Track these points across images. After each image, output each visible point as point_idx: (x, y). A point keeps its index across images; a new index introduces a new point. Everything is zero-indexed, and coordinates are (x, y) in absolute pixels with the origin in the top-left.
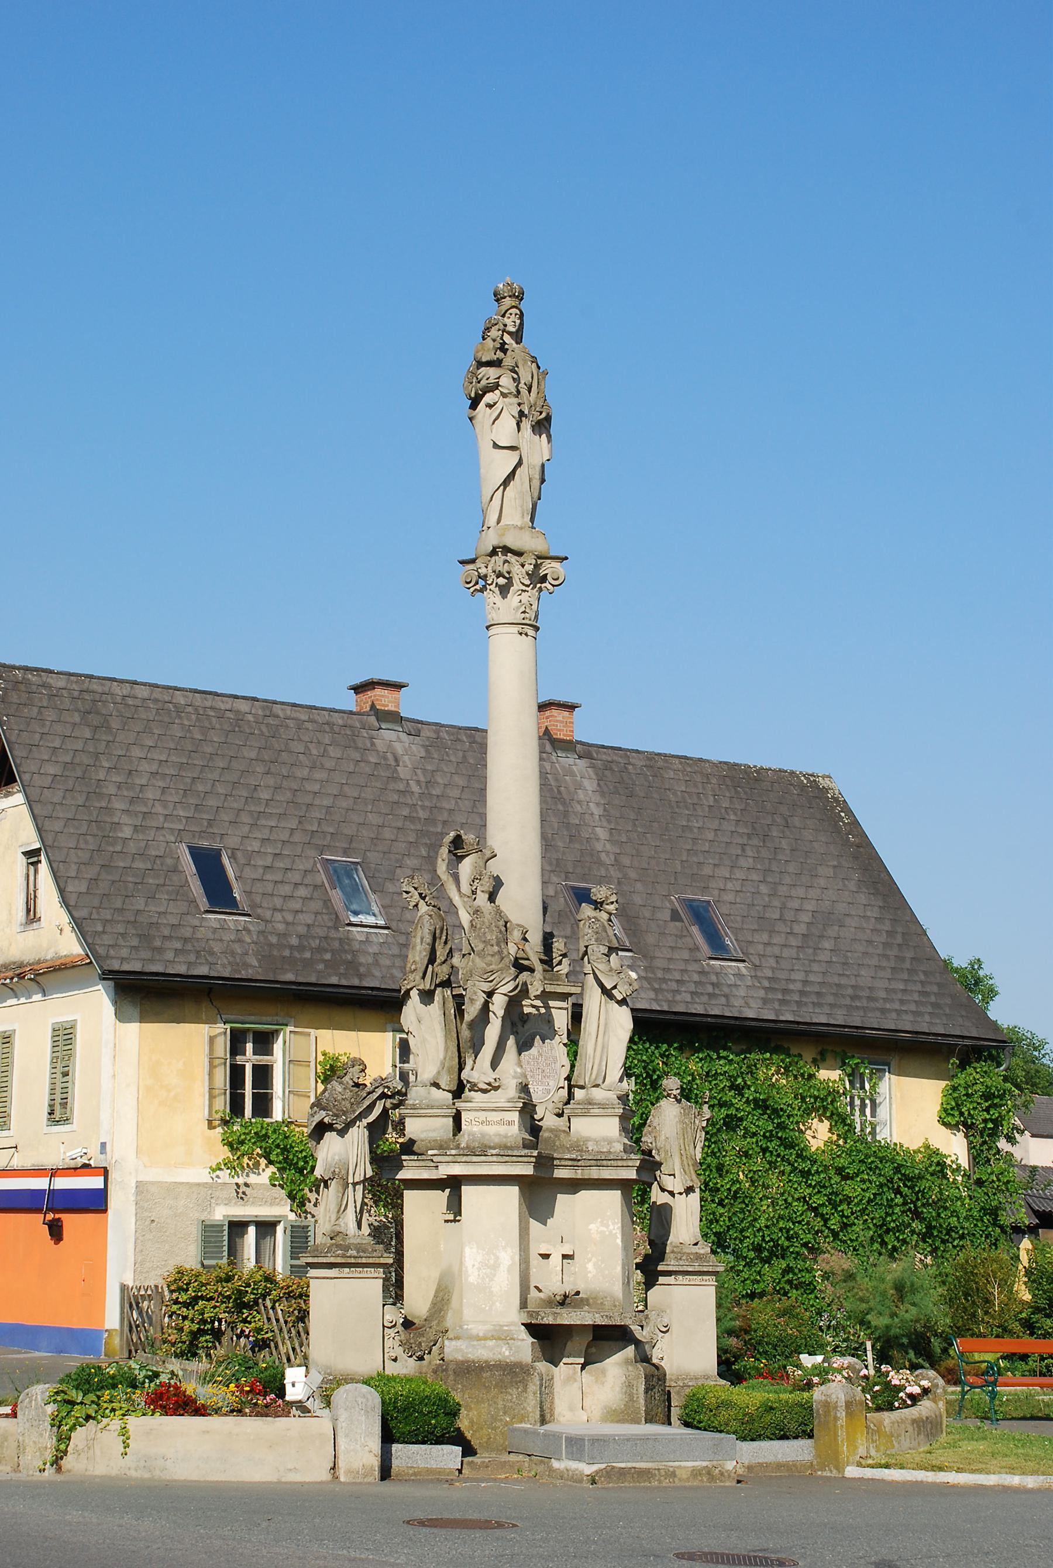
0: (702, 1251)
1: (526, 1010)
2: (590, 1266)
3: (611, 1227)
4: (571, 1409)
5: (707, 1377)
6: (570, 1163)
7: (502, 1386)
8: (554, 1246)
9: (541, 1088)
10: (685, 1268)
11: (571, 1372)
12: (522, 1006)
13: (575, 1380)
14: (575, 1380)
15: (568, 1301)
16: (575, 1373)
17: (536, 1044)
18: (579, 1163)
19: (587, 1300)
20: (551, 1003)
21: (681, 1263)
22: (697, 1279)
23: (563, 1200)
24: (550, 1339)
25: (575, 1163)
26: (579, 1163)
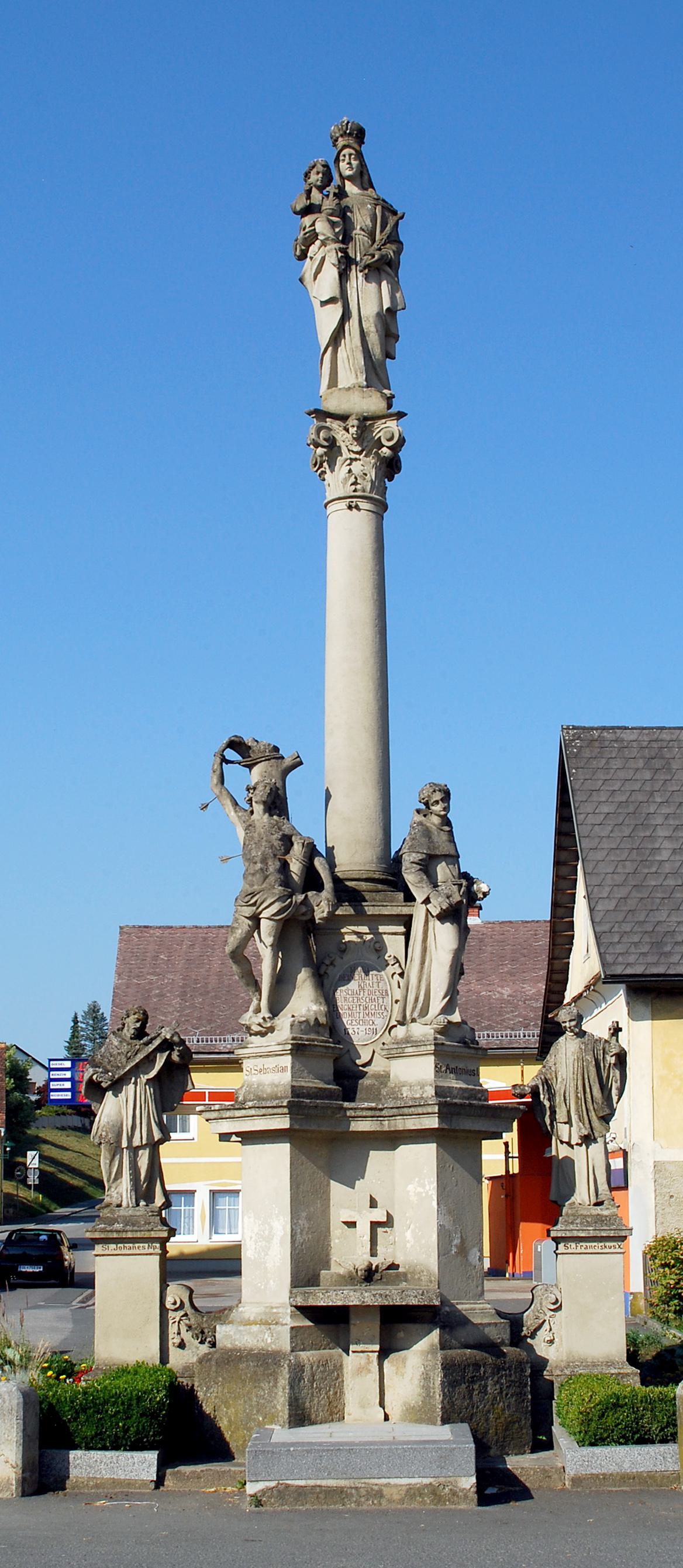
0: (606, 1213)
1: (347, 938)
2: (408, 1235)
3: (427, 1188)
4: (363, 1406)
5: (610, 1364)
6: (369, 1113)
7: (255, 1379)
8: (360, 1212)
9: (362, 1028)
10: (575, 1234)
11: (363, 1362)
12: (342, 935)
13: (369, 1371)
14: (369, 1371)
15: (377, 1276)
16: (369, 1362)
17: (356, 977)
18: (384, 1113)
19: (405, 1274)
20: (382, 929)
21: (572, 1227)
22: (597, 1246)
23: (377, 1159)
24: (330, 1323)
25: (378, 1113)
26: (384, 1113)
